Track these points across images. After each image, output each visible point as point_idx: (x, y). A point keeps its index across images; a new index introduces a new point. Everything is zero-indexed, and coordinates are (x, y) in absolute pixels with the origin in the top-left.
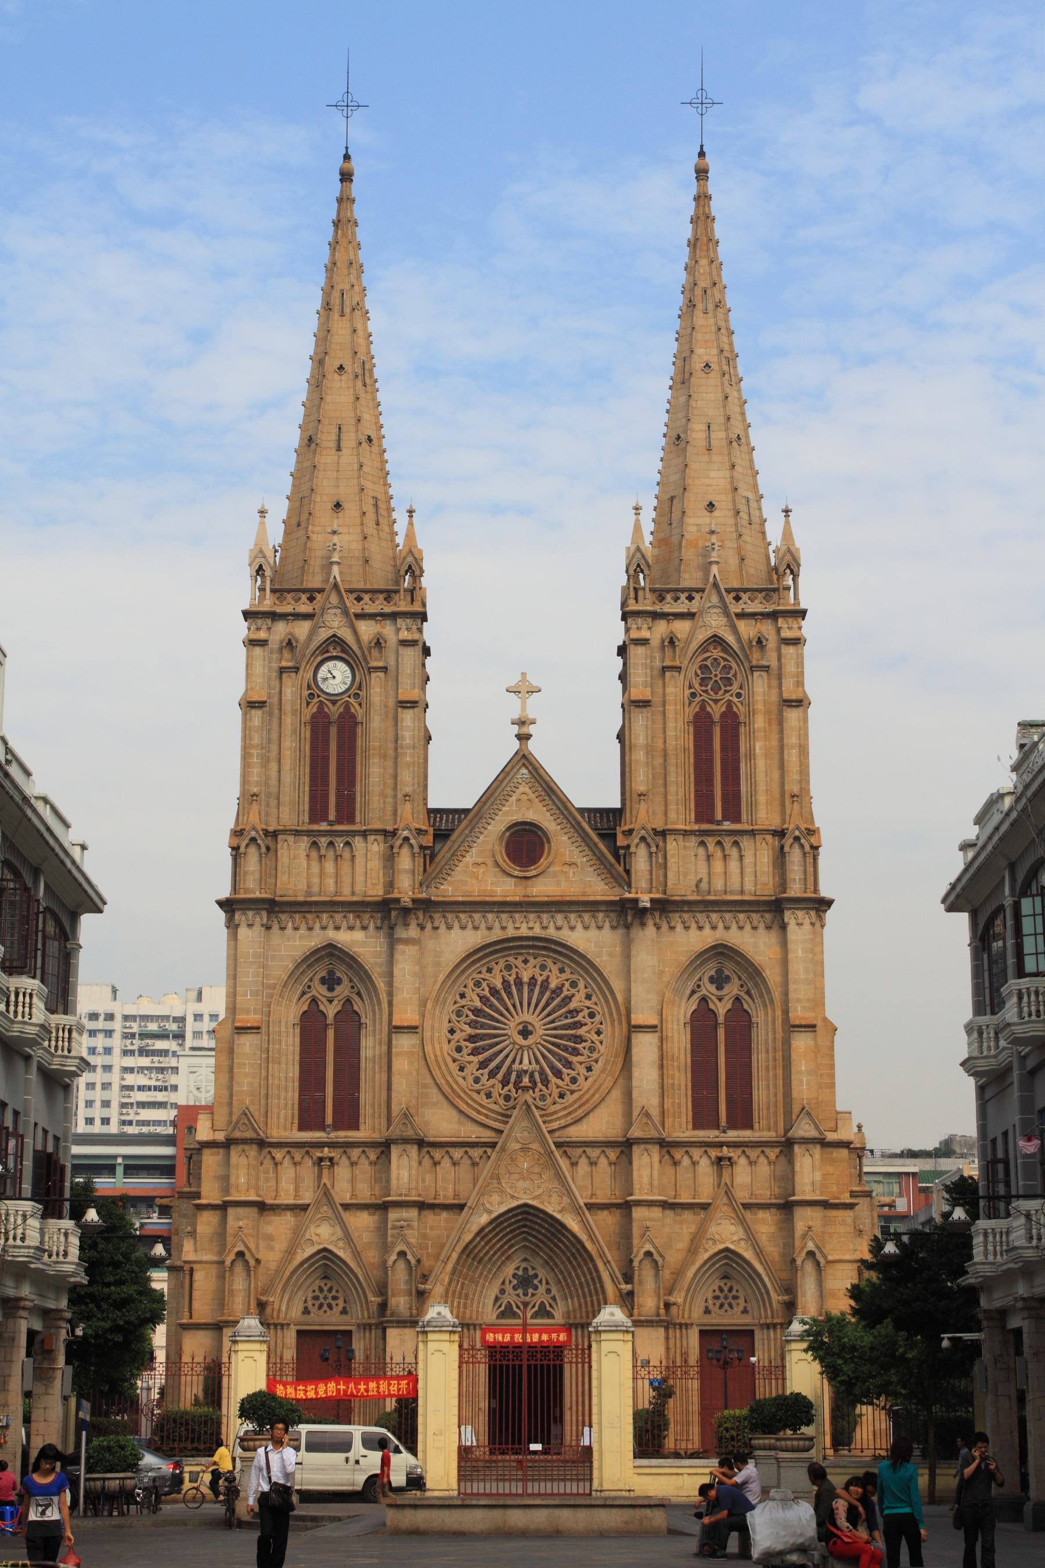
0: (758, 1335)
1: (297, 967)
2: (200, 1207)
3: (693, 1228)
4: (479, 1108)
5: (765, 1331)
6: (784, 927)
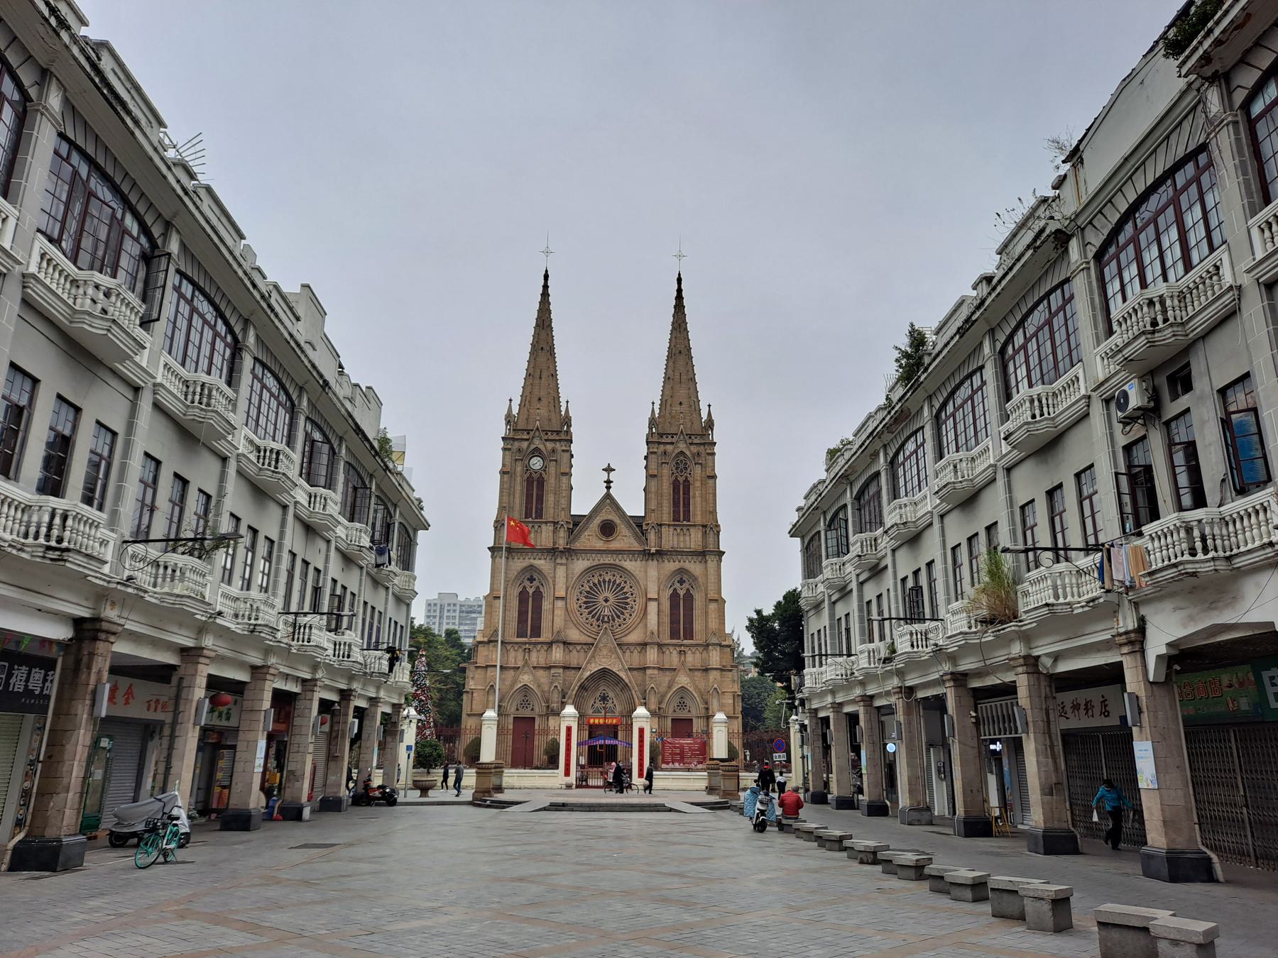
0: (695, 721)
1: (519, 573)
2: (477, 667)
6: (706, 562)
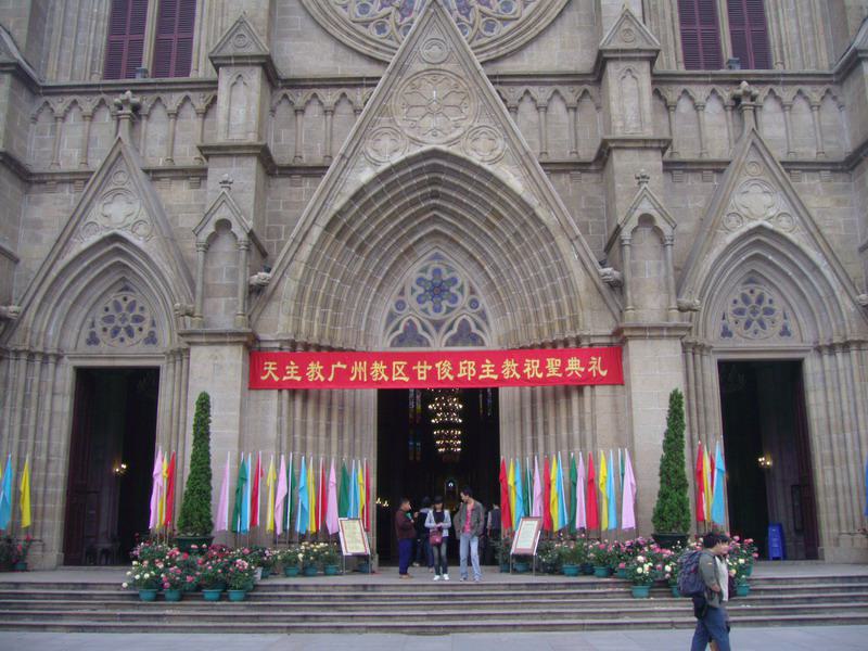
0: (812, 367)
4: (364, 40)
5: (826, 357)
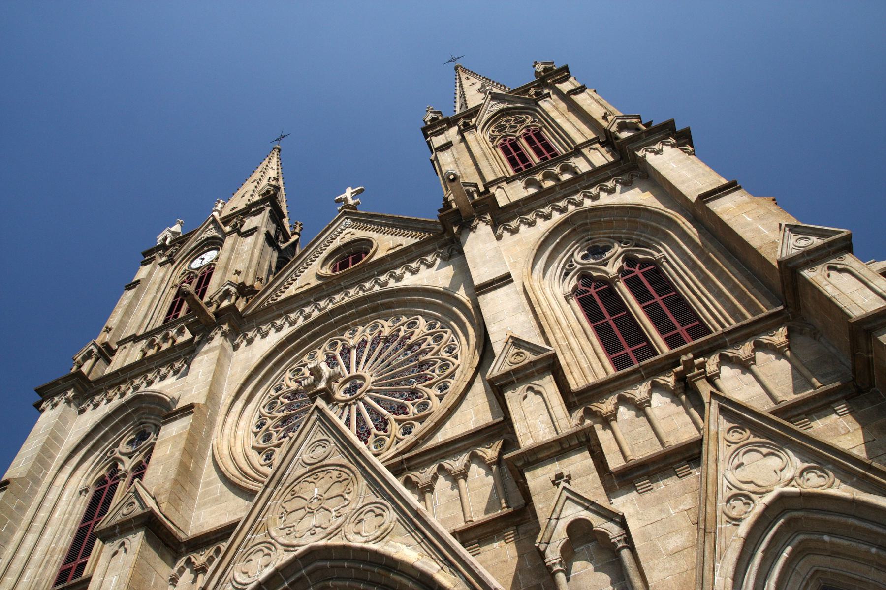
3: (688, 502)
